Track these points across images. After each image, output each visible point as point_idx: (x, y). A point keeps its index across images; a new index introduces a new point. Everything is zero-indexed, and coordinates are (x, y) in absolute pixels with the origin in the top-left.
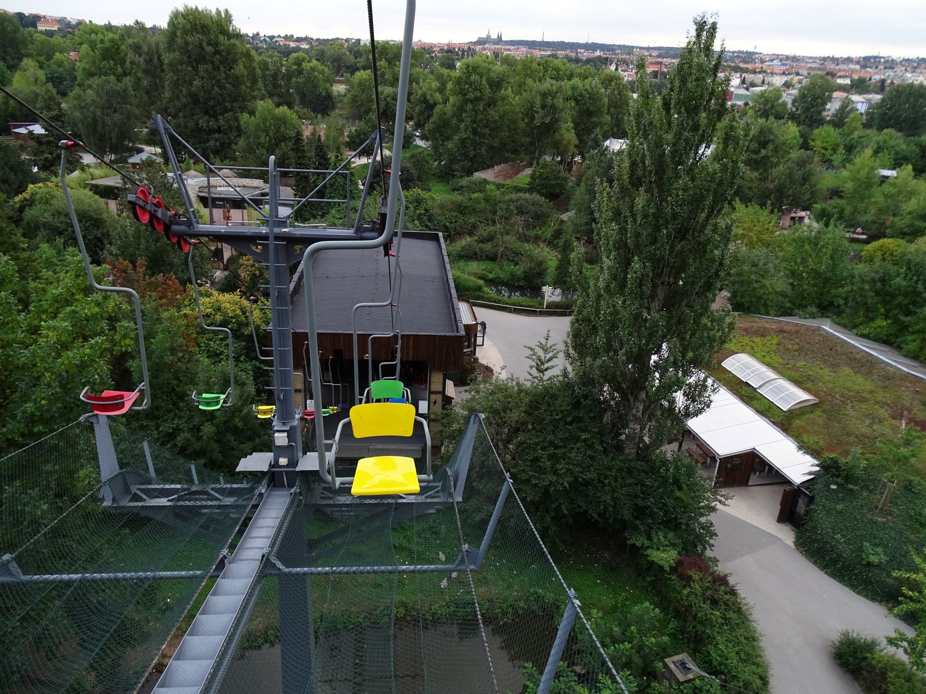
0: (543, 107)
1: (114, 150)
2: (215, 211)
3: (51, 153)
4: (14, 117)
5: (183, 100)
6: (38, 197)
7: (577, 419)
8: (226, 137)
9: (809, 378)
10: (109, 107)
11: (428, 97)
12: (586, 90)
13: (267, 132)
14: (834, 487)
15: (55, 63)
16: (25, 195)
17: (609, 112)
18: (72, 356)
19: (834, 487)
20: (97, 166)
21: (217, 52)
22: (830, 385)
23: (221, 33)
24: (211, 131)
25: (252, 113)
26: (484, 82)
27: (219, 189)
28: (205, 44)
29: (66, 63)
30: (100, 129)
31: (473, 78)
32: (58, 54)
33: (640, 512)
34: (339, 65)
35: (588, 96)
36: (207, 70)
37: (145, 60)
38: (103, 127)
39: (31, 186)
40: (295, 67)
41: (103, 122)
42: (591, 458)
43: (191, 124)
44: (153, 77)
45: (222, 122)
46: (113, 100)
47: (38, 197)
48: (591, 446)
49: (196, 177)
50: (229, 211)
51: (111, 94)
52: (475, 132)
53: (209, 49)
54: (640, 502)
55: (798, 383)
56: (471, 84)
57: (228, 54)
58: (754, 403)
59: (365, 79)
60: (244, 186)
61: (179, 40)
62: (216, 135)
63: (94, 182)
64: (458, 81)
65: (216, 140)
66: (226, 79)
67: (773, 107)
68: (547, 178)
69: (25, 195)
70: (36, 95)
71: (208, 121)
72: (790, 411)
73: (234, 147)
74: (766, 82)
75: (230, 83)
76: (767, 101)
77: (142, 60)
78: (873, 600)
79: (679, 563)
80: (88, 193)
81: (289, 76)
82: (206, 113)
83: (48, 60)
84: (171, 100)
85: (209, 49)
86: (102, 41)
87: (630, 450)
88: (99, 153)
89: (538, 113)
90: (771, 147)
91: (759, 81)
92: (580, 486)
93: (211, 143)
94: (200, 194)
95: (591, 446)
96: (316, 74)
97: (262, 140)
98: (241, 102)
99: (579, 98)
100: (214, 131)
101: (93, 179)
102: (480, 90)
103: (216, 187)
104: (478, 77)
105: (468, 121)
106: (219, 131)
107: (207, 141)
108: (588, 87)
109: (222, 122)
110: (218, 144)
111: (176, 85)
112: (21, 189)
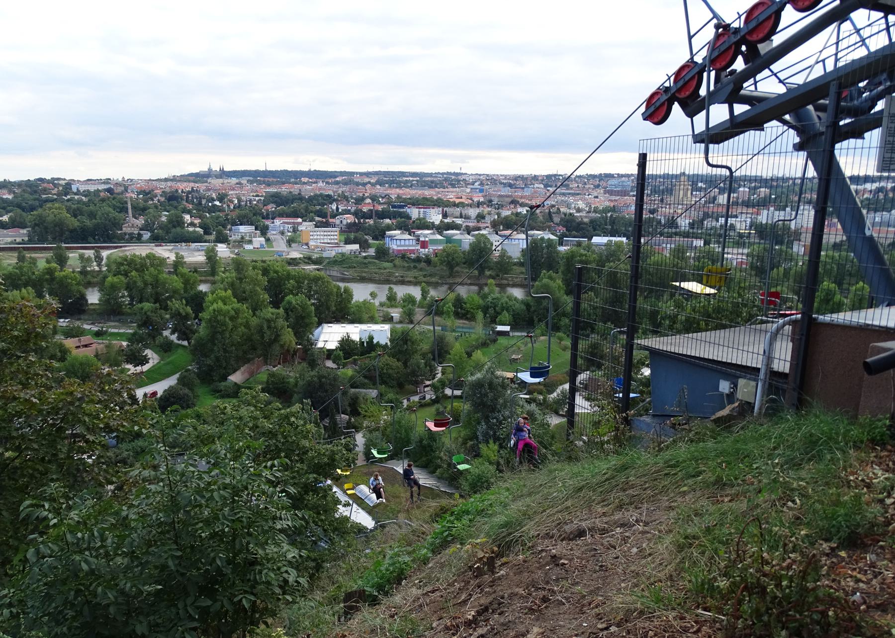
11: (181, 311)
12: (298, 304)
17: (316, 316)
26: (227, 319)
34: (61, 229)
64: (210, 320)
67: (453, 259)
68: (277, 383)
74: (463, 214)
76: (448, 255)
91: (458, 214)
96: (70, 281)
102: (225, 325)
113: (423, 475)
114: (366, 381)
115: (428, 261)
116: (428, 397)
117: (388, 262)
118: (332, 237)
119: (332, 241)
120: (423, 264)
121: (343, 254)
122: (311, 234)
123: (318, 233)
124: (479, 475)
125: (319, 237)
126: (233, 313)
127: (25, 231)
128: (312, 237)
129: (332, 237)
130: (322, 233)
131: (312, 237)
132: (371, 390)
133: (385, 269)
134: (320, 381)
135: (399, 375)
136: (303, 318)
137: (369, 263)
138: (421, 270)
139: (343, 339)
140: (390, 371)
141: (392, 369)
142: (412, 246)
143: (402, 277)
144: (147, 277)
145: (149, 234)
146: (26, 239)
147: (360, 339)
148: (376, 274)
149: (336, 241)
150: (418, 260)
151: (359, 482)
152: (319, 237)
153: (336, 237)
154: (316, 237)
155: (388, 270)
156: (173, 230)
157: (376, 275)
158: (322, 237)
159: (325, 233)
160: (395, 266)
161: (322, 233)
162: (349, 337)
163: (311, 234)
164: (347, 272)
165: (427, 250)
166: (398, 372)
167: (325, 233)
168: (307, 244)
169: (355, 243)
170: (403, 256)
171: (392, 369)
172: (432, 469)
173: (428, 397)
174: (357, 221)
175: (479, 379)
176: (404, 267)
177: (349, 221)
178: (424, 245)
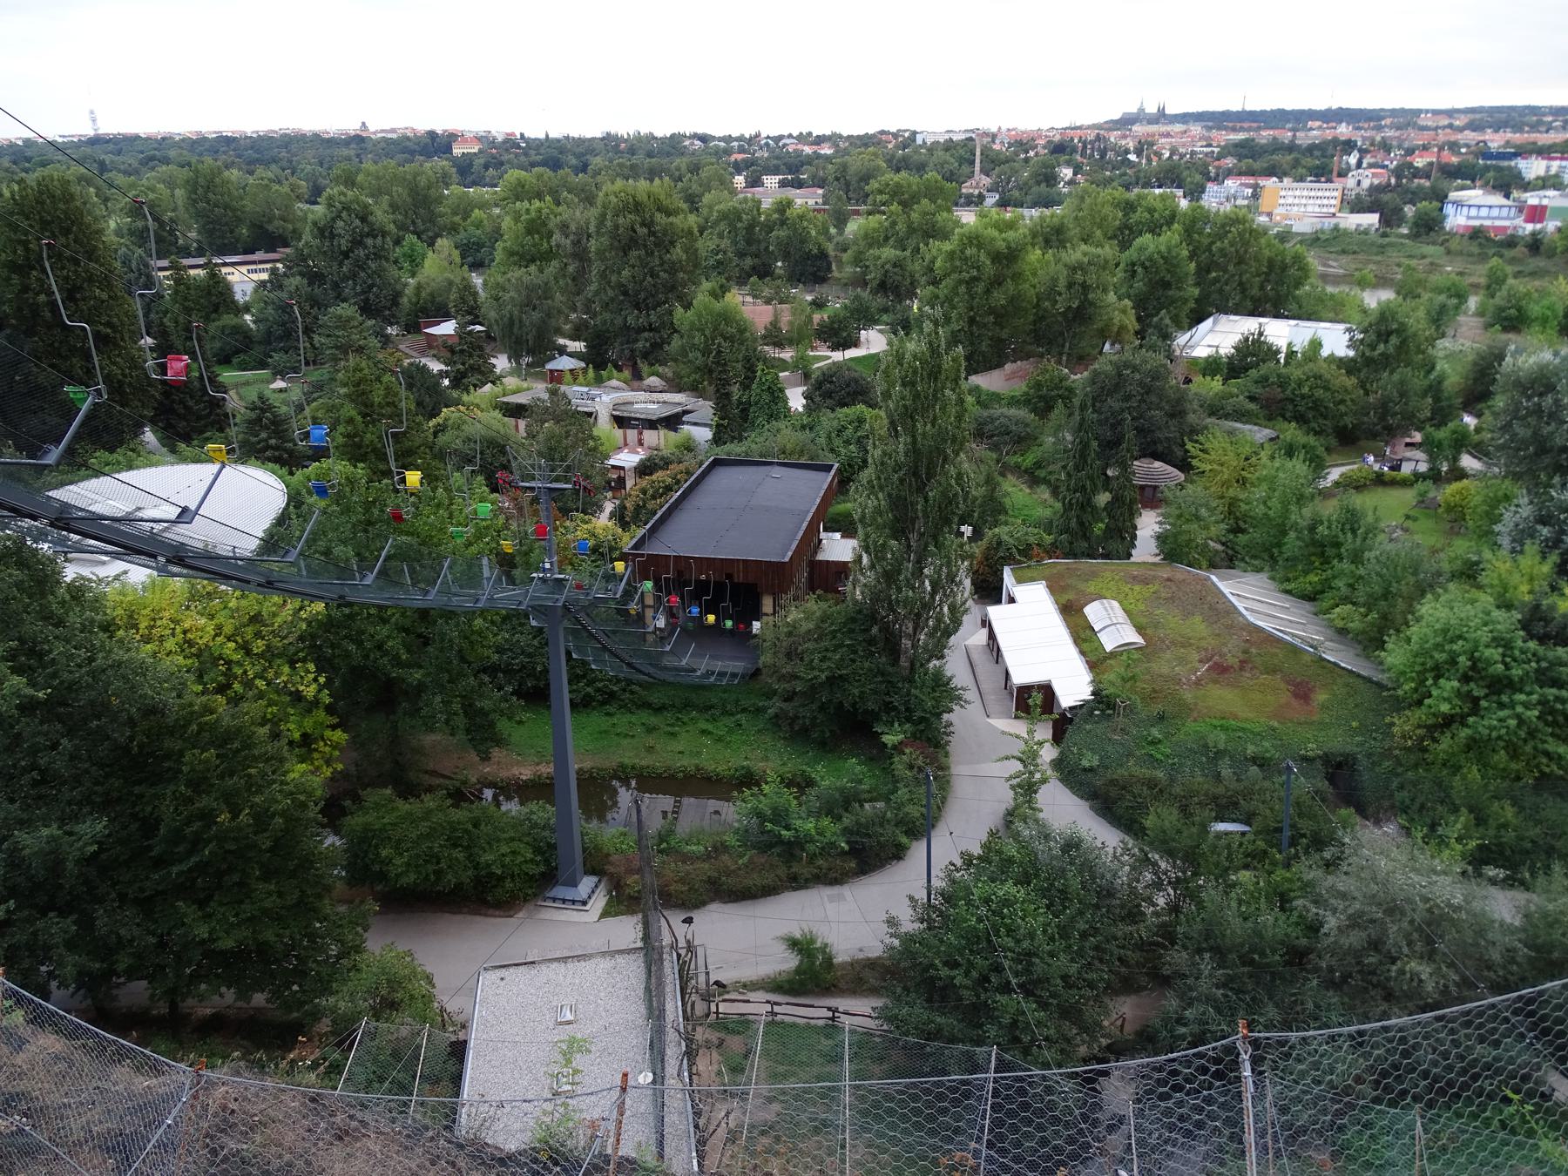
0: (1070, 286)
1: (530, 352)
2: (629, 432)
3: (463, 364)
4: (425, 311)
5: (611, 293)
6: (450, 422)
7: (852, 631)
8: (657, 335)
9: (1156, 626)
10: (528, 304)
12: (1159, 252)
13: (702, 330)
14: (1097, 712)
15: (473, 224)
16: (439, 420)
18: (474, 549)
19: (1097, 712)
20: (512, 373)
21: (653, 234)
22: (1169, 632)
23: (659, 209)
24: (640, 330)
25: (688, 306)
27: (636, 406)
28: (637, 227)
29: (485, 222)
30: (515, 330)
31: (968, 252)
32: (477, 211)
33: (888, 707)
35: (1162, 261)
36: (639, 257)
37: (572, 242)
38: (520, 328)
39: (444, 410)
40: (776, 216)
41: (520, 322)
42: (853, 661)
43: (619, 321)
44: (581, 260)
45: (653, 318)
46: (534, 297)
47: (450, 422)
48: (855, 652)
49: (617, 389)
50: (641, 433)
51: (531, 289)
52: (972, 321)
53: (642, 231)
54: (888, 699)
55: (1140, 629)
56: (966, 259)
57: (664, 235)
58: (1085, 646)
59: (874, 229)
60: (664, 402)
61: (609, 223)
62: (646, 334)
63: (505, 399)
65: (646, 340)
66: (661, 265)
69: (439, 420)
70: (451, 283)
71: (638, 318)
72: (1111, 653)
73: (666, 348)
75: (665, 271)
77: (568, 241)
78: (1082, 798)
79: (901, 743)
80: (497, 414)
81: (769, 227)
82: (637, 306)
83: (464, 219)
84: (597, 293)
85: (642, 231)
86: (528, 211)
87: (904, 662)
88: (515, 356)
89: (1060, 294)
90: (1394, 340)
92: (834, 681)
93: (640, 345)
94: (615, 413)
95: (855, 652)
96: (805, 224)
97: (696, 341)
98: (676, 291)
99: (1147, 264)
100: (644, 330)
101: (504, 395)
102: (978, 268)
103: (632, 403)
104: (974, 250)
105: (962, 307)
106: (651, 330)
107: (636, 341)
108: (1163, 248)
109: (653, 318)
110: (648, 345)
111: (603, 275)
112: (434, 413)
113: (1293, 614)
114: (1252, 406)
115: (1535, 245)
116: (1407, 469)
117: (1434, 243)
118: (1325, 202)
119: (1325, 210)
120: (1520, 251)
121: (1336, 228)
122: (1283, 193)
123: (1298, 193)
124: (1445, 631)
125: (1296, 201)
126: (1001, 245)
127: (820, 191)
128: (1282, 201)
129: (1325, 202)
130: (1305, 193)
131: (1282, 201)
132: (1256, 428)
133: (1424, 257)
134: (1120, 375)
135: (1342, 408)
136: (1166, 285)
137: (1391, 245)
138: (1512, 261)
139: (1247, 339)
140: (1319, 393)
141: (1326, 389)
142: (1508, 218)
143: (1461, 274)
144: (915, 216)
145: (997, 197)
146: (820, 201)
147: (1290, 345)
148: (1399, 265)
149: (1332, 210)
150: (1511, 242)
151: (1108, 596)
152: (1296, 201)
153: (1333, 202)
154: (1290, 201)
155: (1427, 261)
156: (1035, 189)
157: (1396, 269)
158: (1304, 201)
159: (1312, 194)
160: (1449, 252)
161: (1305, 193)
162: (1261, 334)
163: (1283, 193)
164: (1335, 260)
165: (1539, 226)
166: (1342, 401)
167: (1312, 194)
168: (1270, 214)
169: (1371, 210)
170: (1476, 234)
171: (1326, 389)
172: (1325, 605)
173: (1407, 469)
174: (1393, 181)
175: (1543, 368)
176: (1470, 255)
177: (1376, 182)
178: (1536, 214)
